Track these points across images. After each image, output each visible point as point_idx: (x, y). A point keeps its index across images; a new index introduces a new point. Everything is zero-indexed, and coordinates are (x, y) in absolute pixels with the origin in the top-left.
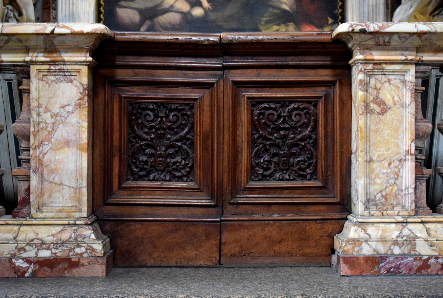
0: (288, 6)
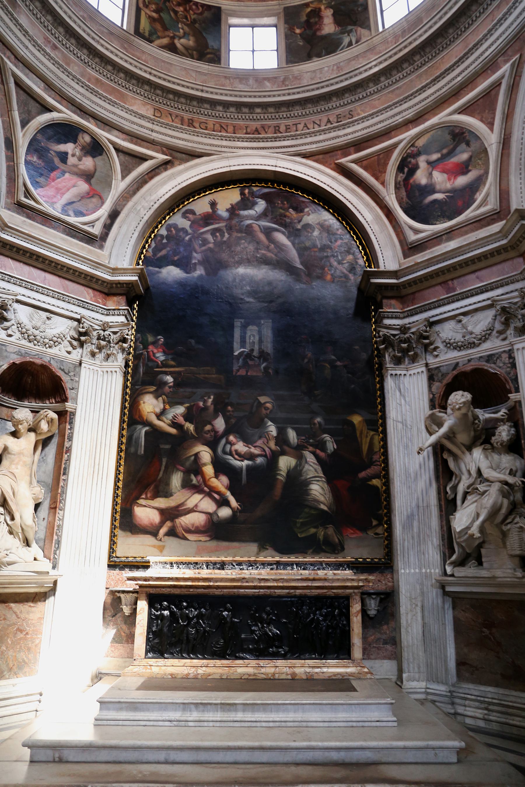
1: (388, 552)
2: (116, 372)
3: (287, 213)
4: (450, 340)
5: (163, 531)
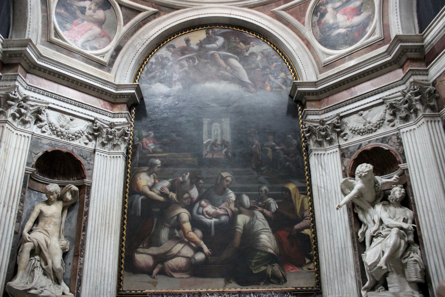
0: (272, 250)
1: (318, 282)
2: (120, 157)
3: (239, 46)
4: (355, 128)
5: (155, 271)
